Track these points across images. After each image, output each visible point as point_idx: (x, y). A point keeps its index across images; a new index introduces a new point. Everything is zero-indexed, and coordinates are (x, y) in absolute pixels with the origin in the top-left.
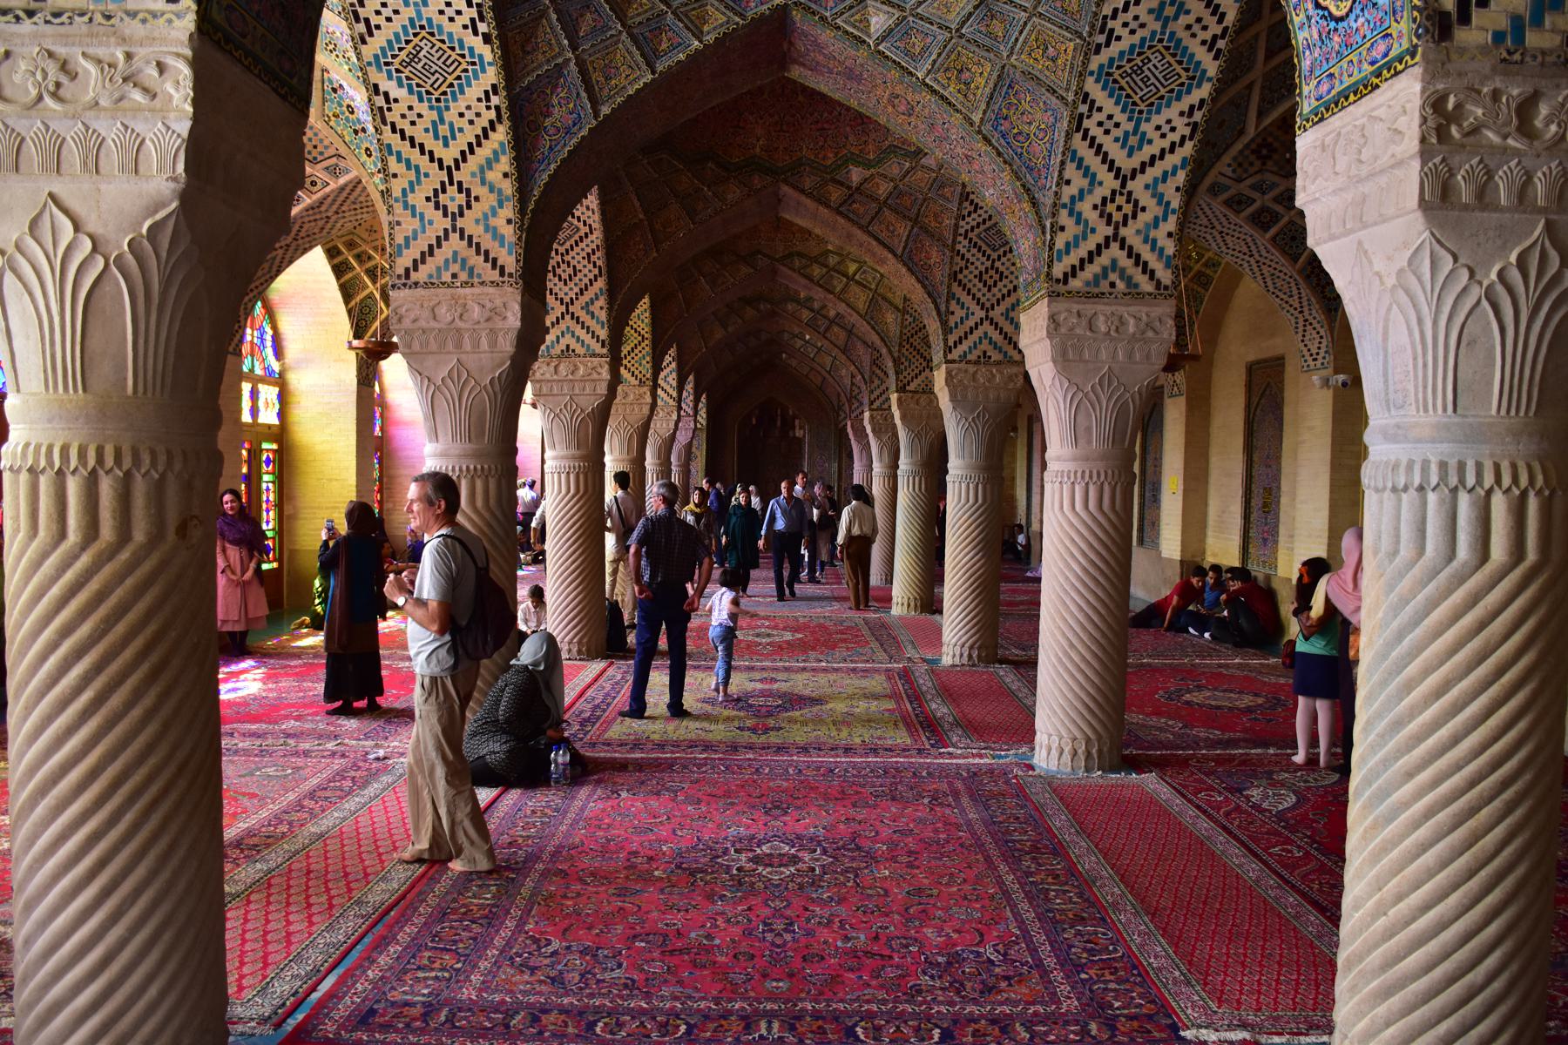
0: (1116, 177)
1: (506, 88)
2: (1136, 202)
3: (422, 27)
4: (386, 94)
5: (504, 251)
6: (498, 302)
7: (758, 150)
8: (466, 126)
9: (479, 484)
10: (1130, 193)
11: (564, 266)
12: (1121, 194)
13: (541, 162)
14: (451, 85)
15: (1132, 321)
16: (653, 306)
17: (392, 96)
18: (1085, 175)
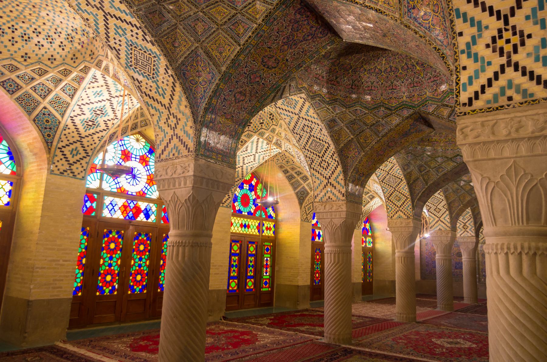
0: (499, 18)
1: (171, 65)
2: (522, 33)
3: (131, 45)
4: (137, 79)
5: (190, 141)
6: (187, 164)
7: (404, 98)
8: (167, 87)
9: (180, 249)
10: (514, 27)
11: (323, 162)
12: (507, 30)
13: (201, 98)
14: (154, 70)
15: (530, 123)
16: (408, 183)
17: (140, 80)
18: (472, 25)
